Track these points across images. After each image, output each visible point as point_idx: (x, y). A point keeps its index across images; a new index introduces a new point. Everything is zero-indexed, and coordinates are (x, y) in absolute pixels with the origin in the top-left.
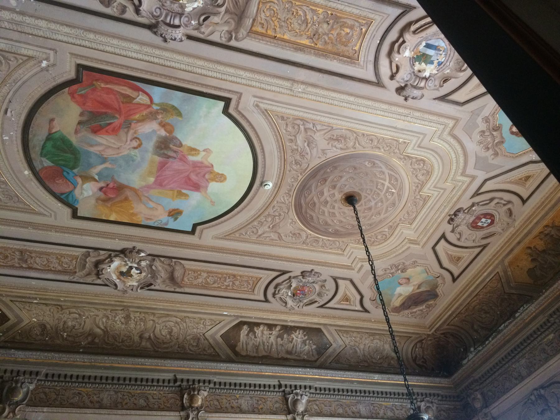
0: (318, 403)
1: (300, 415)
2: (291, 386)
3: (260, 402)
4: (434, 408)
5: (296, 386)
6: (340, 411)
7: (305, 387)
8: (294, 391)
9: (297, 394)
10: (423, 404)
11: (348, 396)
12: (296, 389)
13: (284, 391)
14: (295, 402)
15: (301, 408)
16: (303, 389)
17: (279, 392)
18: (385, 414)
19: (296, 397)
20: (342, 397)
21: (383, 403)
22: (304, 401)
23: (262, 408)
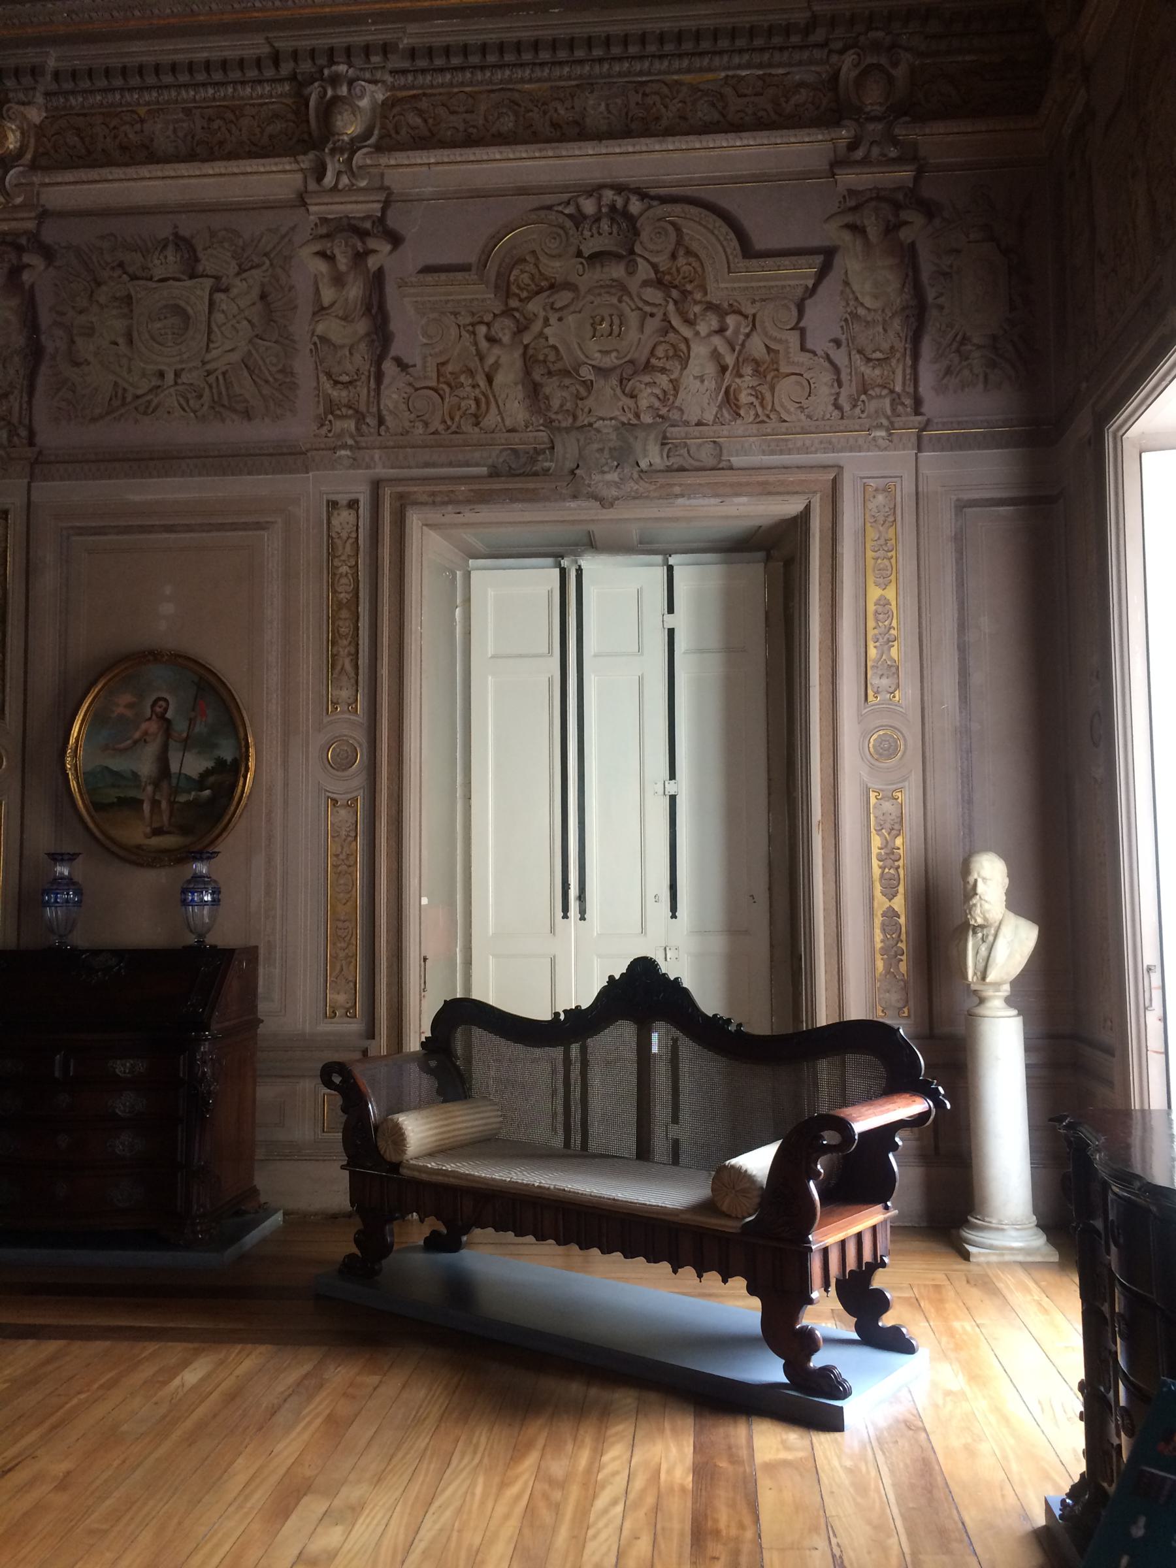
0: (424, 104)
1: (342, 151)
2: (312, 53)
3: (215, 125)
4: (899, 72)
5: (331, 52)
6: (507, 123)
7: (367, 50)
8: (326, 72)
9: (335, 80)
10: (849, 58)
11: (542, 64)
12: (332, 62)
13: (293, 77)
14: (329, 108)
15: (349, 127)
16: (358, 61)
17: (280, 80)
18: (683, 118)
19: (330, 93)
20: (519, 73)
21: (687, 78)
22: (364, 103)
23: (221, 143)
